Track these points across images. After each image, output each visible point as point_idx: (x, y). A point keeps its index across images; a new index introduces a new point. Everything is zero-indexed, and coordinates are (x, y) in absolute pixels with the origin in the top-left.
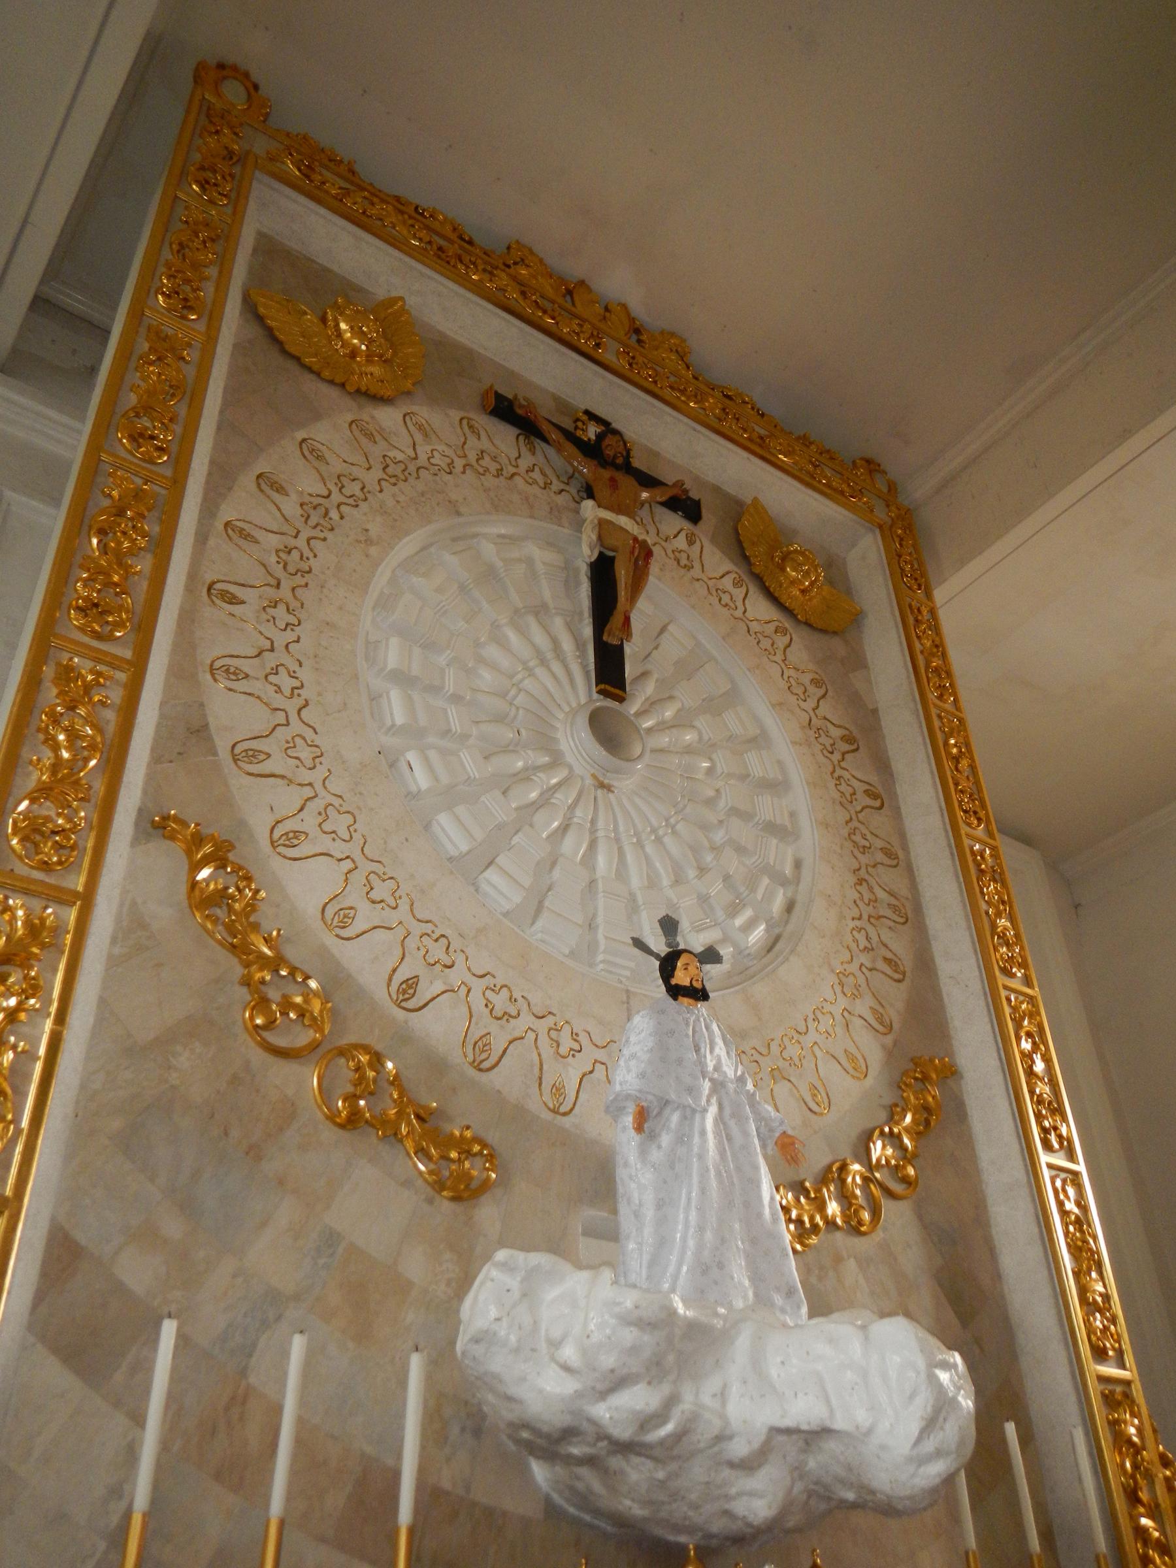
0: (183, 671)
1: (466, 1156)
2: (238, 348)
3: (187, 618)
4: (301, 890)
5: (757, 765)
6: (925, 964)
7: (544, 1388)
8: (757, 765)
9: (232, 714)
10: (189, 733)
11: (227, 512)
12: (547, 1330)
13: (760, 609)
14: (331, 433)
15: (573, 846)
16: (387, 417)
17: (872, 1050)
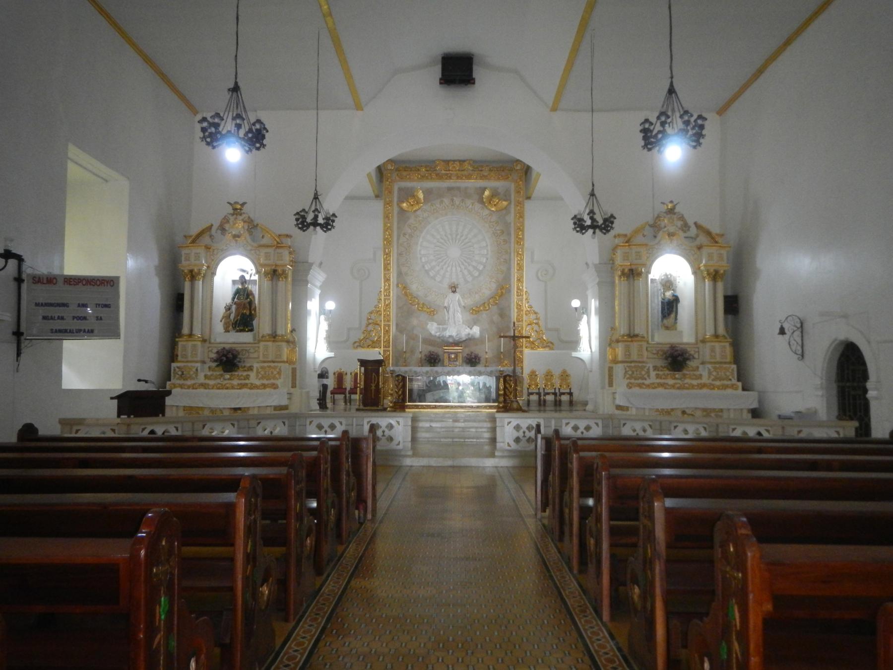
0: (398, 266)
1: (432, 312)
2: (398, 213)
3: (398, 259)
4: (414, 287)
5: (484, 244)
6: (509, 269)
7: (433, 333)
8: (484, 244)
9: (404, 269)
10: (400, 274)
11: (401, 241)
12: (433, 328)
13: (486, 212)
14: (412, 221)
15: (449, 269)
16: (419, 213)
17: (494, 286)
